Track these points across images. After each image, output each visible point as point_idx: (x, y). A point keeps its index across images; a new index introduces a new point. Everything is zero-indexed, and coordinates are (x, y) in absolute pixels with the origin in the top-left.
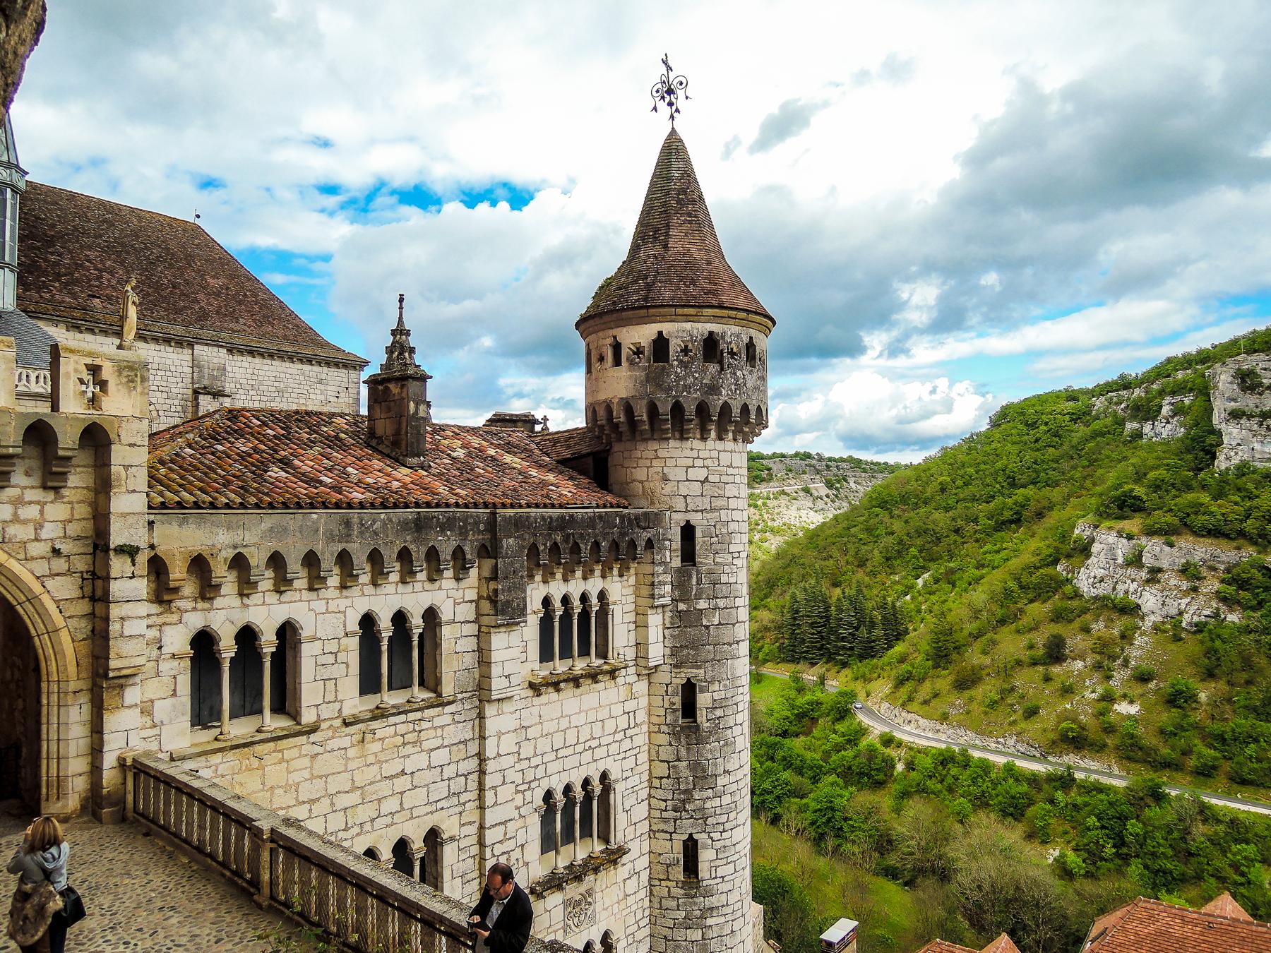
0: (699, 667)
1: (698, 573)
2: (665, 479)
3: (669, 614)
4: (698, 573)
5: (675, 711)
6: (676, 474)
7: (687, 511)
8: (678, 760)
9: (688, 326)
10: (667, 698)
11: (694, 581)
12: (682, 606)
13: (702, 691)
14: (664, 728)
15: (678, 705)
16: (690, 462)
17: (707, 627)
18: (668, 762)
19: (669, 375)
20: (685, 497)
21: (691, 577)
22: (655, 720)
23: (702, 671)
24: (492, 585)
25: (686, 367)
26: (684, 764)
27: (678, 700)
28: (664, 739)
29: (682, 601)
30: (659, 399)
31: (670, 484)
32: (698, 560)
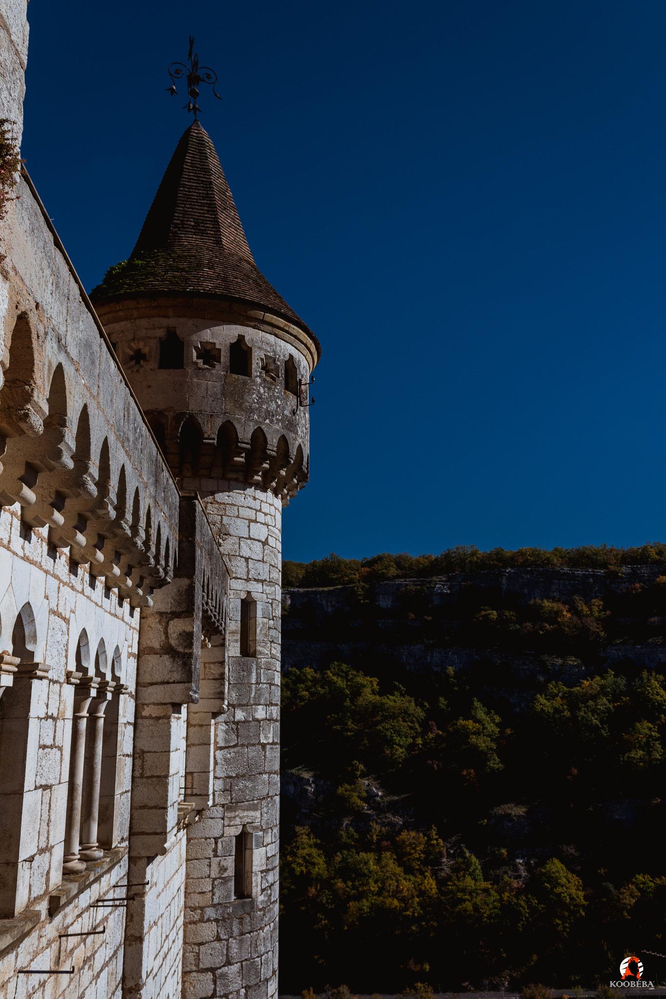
0: (254, 808)
1: (259, 668)
2: (224, 533)
3: (223, 727)
4: (259, 668)
5: (225, 880)
6: (239, 528)
7: (248, 580)
8: (228, 963)
9: (272, 338)
10: (215, 861)
11: (254, 681)
12: (240, 715)
13: (258, 847)
14: (210, 913)
15: (231, 872)
16: (251, 514)
17: (264, 746)
18: (213, 970)
19: (250, 392)
20: (247, 560)
21: (250, 673)
22: (197, 900)
23: (258, 814)
24: (177, 626)
25: (269, 389)
26: (235, 968)
27: (230, 862)
28: (208, 931)
29: (240, 705)
30: (239, 420)
31: (231, 540)
32: (259, 648)
